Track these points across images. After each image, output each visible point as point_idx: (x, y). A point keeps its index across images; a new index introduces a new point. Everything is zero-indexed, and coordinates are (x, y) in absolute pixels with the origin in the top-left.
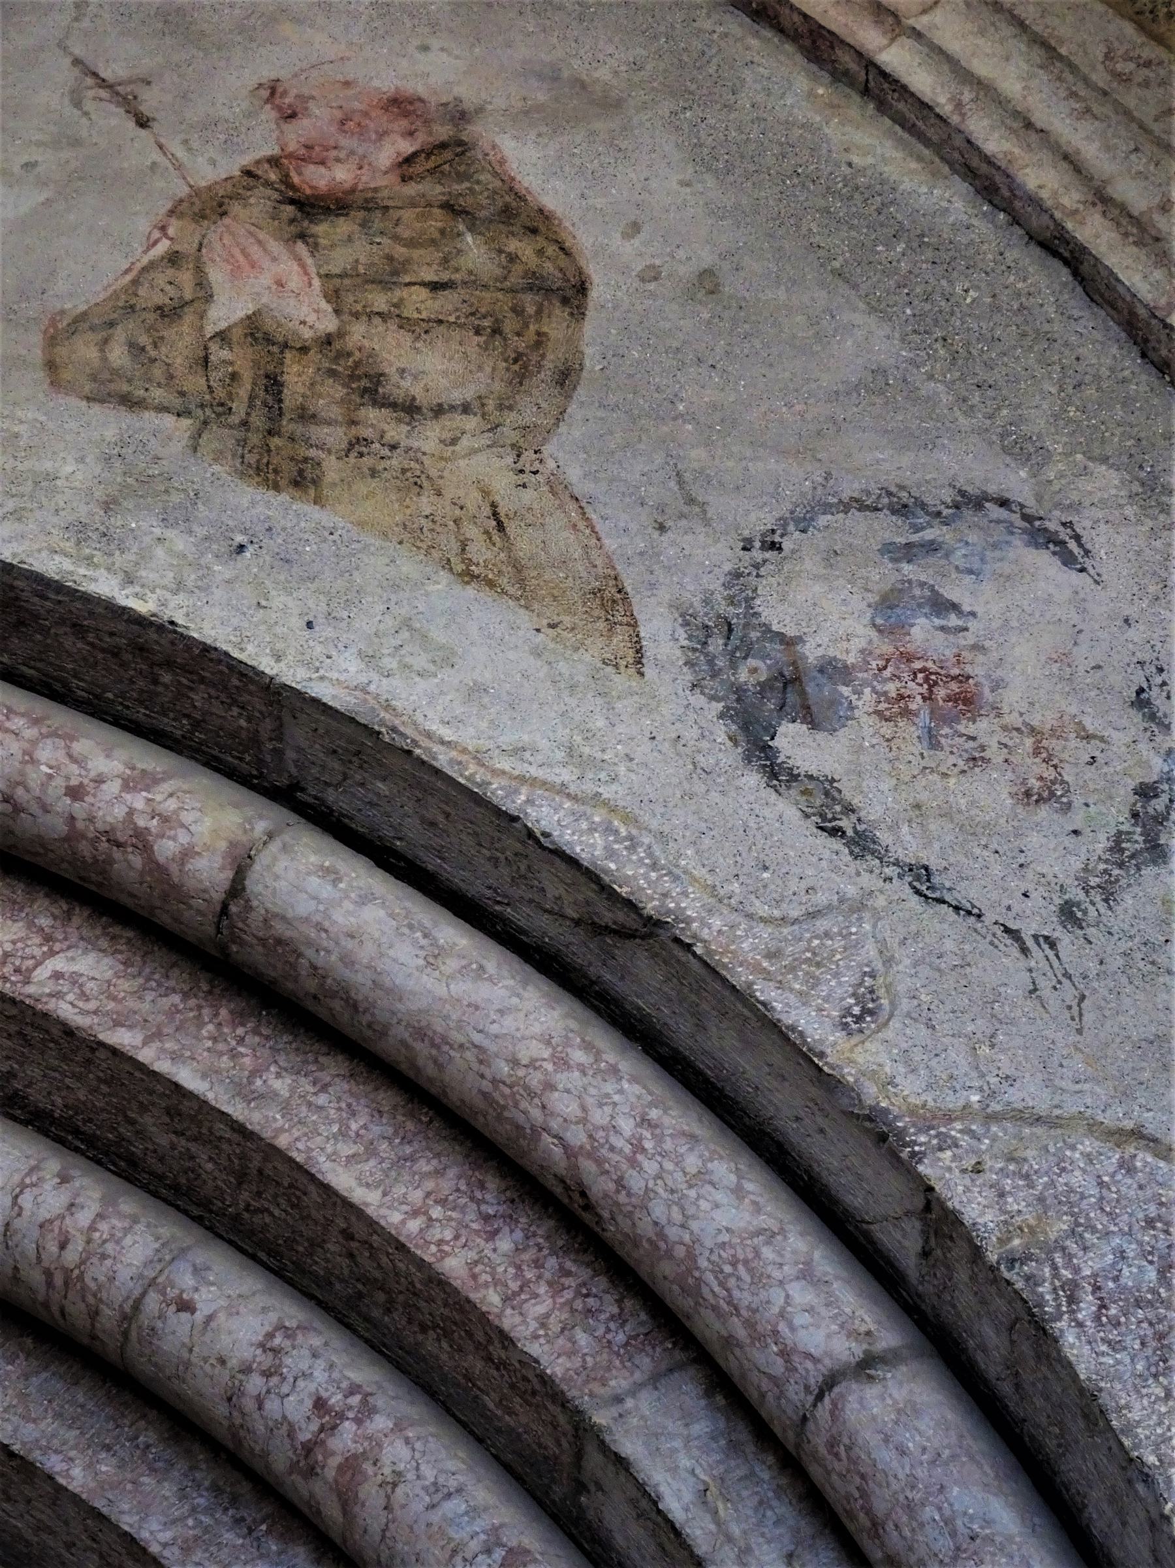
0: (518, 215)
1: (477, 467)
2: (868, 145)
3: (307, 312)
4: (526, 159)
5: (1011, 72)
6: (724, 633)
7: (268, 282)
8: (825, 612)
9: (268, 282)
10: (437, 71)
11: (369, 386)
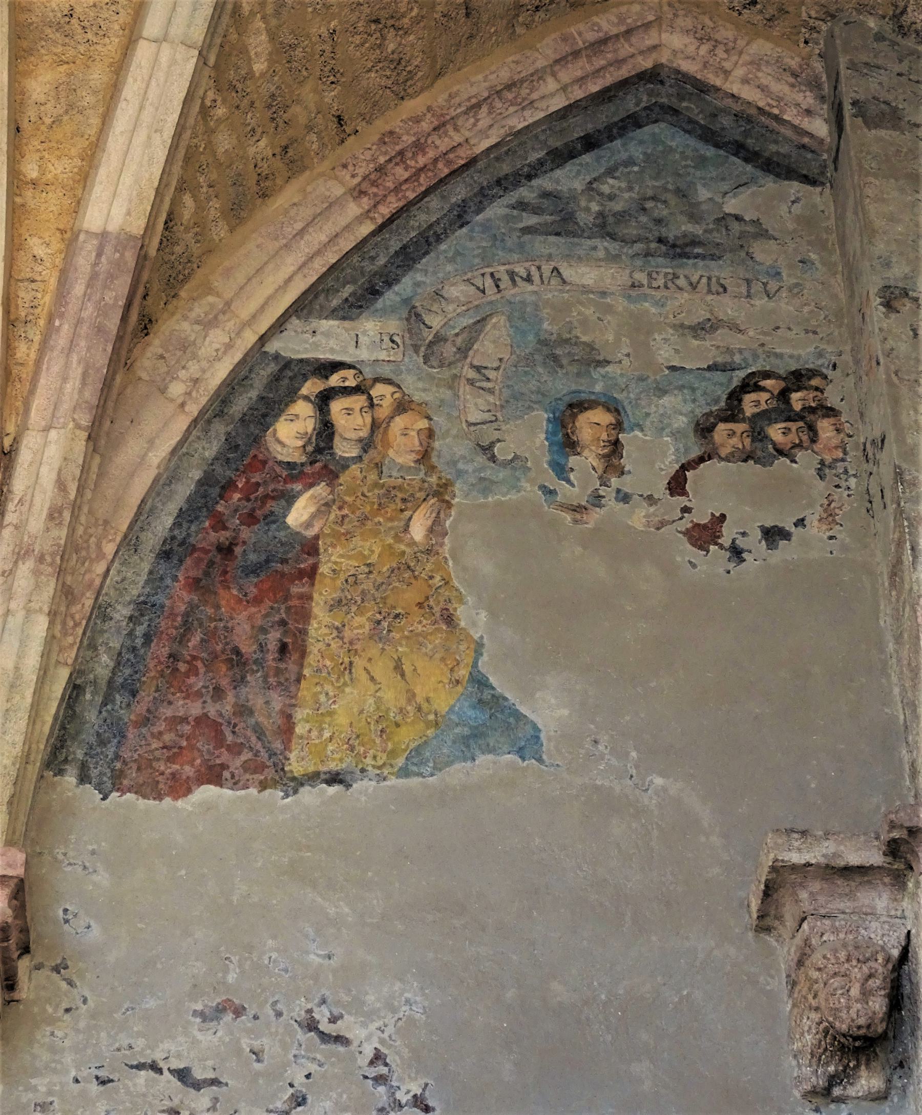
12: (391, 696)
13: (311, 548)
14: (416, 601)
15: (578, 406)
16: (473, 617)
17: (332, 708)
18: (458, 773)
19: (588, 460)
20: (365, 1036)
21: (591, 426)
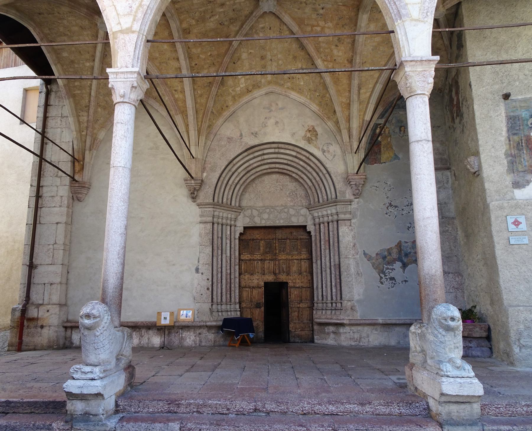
0: (316, 131)
1: (315, 143)
2: (326, 127)
3: (310, 136)
4: (316, 128)
5: (331, 125)
6: (322, 149)
7: (309, 135)
8: (325, 148)
9: (309, 135)
10: (313, 124)
11: (312, 139)
12: (388, 155)
13: (381, 142)
14: (389, 147)
15: (401, 127)
16: (394, 148)
17: (384, 156)
18: (394, 162)
19: (402, 132)
20: (389, 183)
21: (402, 128)
